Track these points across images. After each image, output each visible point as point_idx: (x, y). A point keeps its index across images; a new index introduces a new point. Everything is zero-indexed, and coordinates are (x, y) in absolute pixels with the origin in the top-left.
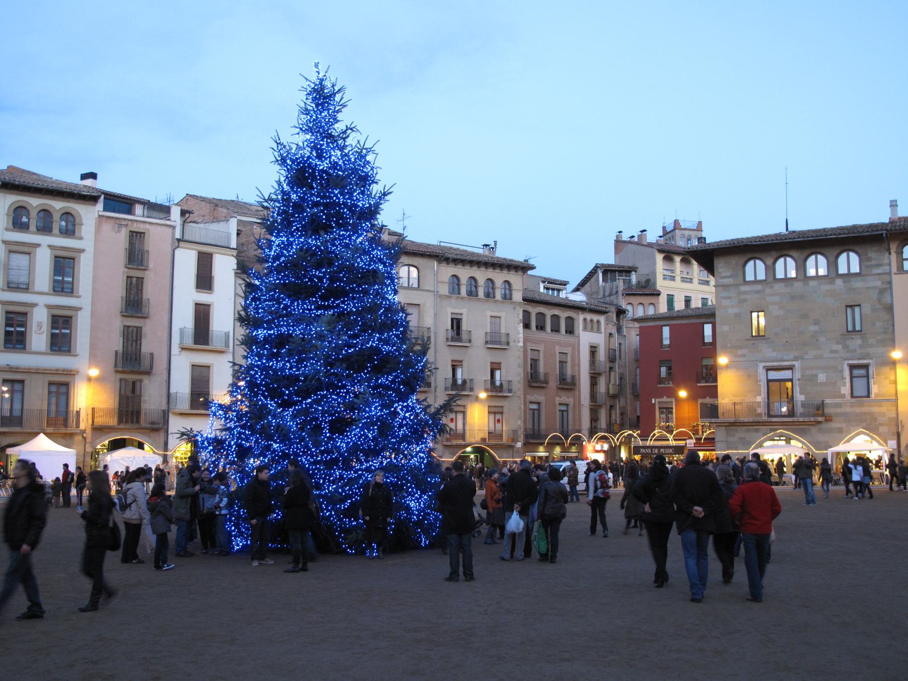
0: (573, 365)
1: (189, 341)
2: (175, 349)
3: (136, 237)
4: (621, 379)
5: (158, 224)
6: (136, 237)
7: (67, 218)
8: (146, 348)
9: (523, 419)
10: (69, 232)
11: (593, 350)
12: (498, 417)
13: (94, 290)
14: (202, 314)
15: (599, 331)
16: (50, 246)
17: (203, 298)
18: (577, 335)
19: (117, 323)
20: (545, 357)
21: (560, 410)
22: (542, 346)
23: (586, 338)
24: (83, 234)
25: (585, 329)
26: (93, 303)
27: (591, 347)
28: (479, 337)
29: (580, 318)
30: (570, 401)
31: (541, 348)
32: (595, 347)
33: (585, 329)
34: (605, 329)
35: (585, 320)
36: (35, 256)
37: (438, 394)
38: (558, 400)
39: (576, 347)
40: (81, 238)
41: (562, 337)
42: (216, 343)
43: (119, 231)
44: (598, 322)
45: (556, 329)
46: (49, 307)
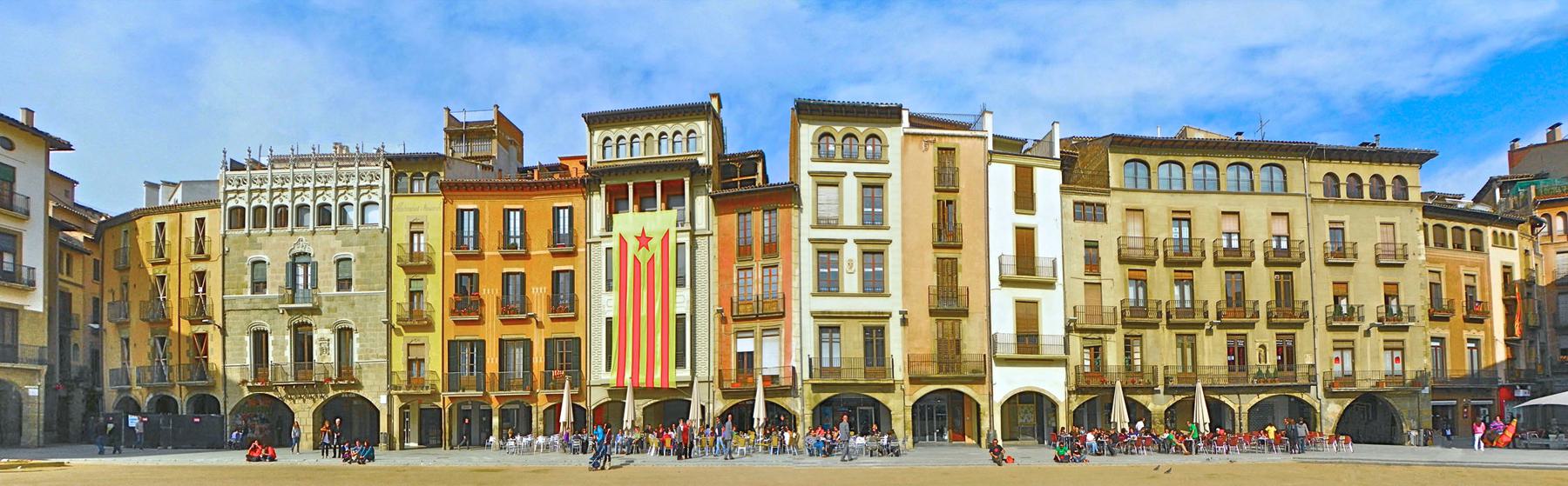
0: (1483, 290)
1: (1011, 272)
2: (995, 282)
3: (946, 152)
4: (1539, 308)
5: (968, 137)
6: (946, 152)
7: (874, 141)
8: (962, 282)
9: (1430, 356)
10: (875, 159)
11: (1507, 271)
12: (1397, 354)
13: (904, 219)
14: (1025, 239)
15: (1512, 246)
16: (855, 174)
17: (1025, 220)
18: (1486, 251)
19: (930, 256)
20: (1447, 280)
21: (1469, 348)
22: (1443, 266)
23: (1498, 257)
24: (890, 157)
25: (1495, 244)
26: (903, 235)
27: (1504, 267)
28: (1366, 253)
29: (1488, 231)
30: (1481, 335)
31: (1442, 268)
32: (1509, 267)
33: (1495, 244)
34: (1520, 245)
35: (1495, 233)
36: (842, 187)
37: (1317, 326)
38: (1466, 335)
39: (1485, 268)
40: (887, 162)
41: (1468, 256)
42: (1044, 274)
43: (926, 150)
44: (1511, 235)
45: (1459, 246)
46: (856, 241)
